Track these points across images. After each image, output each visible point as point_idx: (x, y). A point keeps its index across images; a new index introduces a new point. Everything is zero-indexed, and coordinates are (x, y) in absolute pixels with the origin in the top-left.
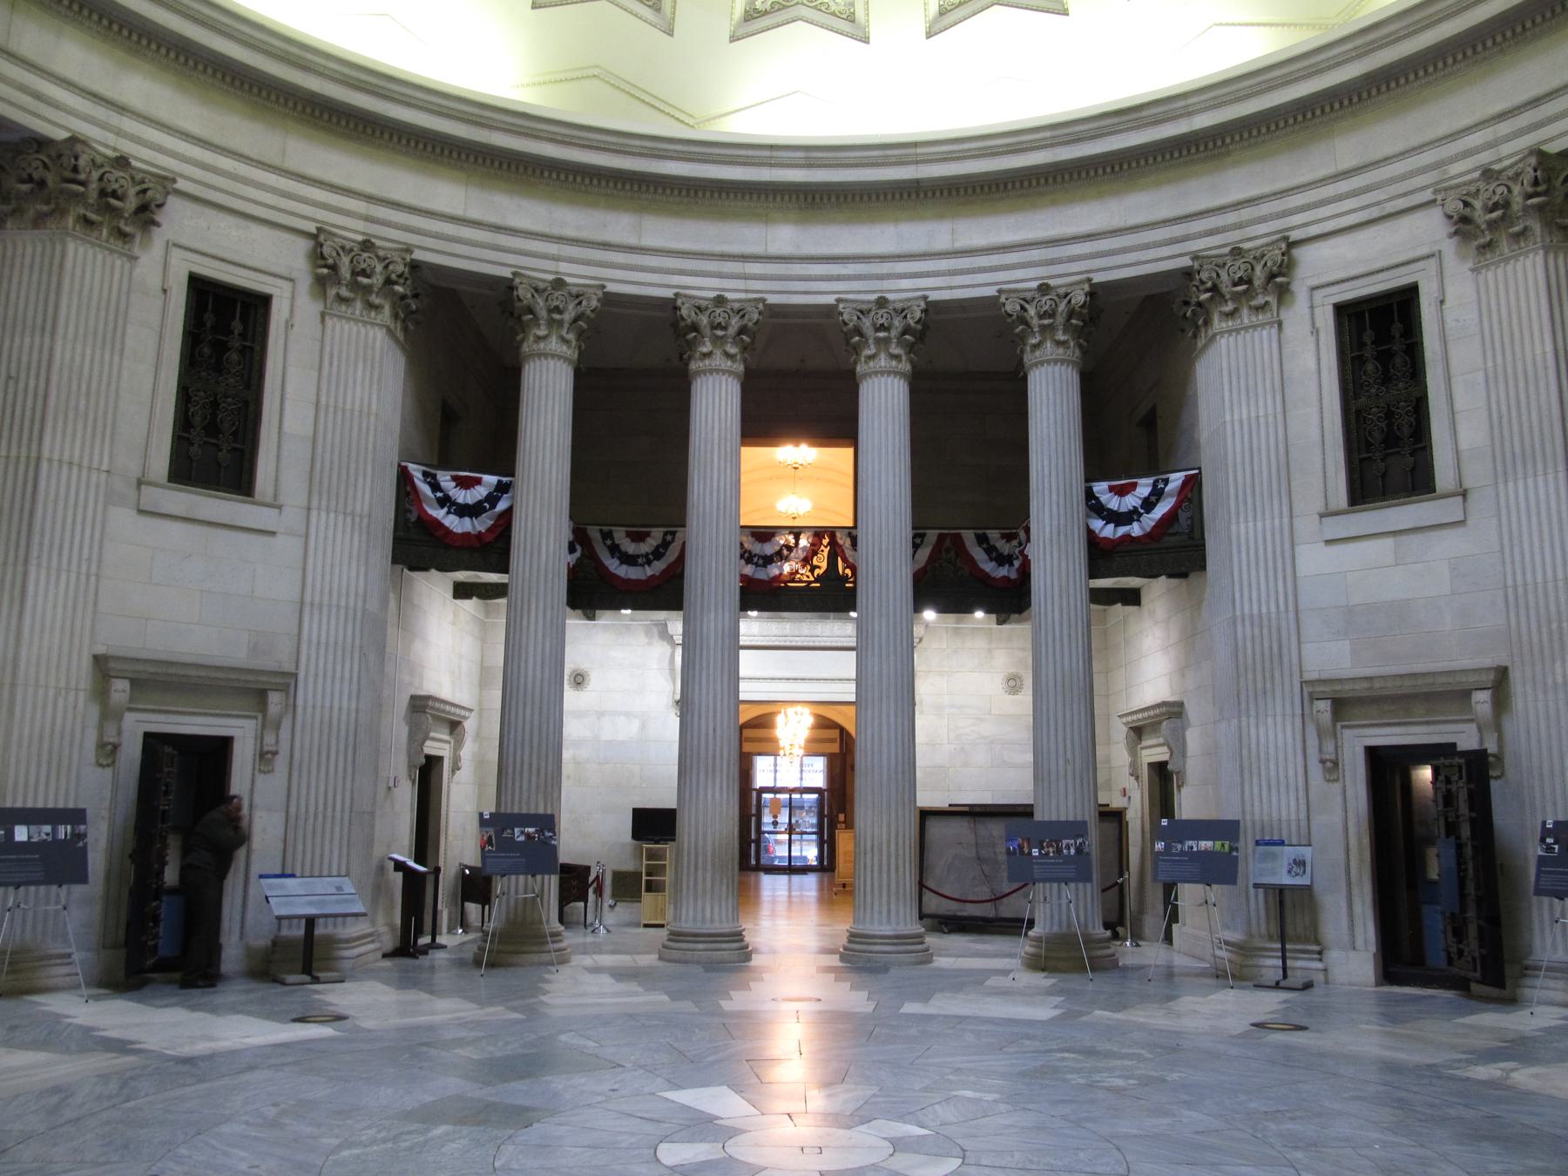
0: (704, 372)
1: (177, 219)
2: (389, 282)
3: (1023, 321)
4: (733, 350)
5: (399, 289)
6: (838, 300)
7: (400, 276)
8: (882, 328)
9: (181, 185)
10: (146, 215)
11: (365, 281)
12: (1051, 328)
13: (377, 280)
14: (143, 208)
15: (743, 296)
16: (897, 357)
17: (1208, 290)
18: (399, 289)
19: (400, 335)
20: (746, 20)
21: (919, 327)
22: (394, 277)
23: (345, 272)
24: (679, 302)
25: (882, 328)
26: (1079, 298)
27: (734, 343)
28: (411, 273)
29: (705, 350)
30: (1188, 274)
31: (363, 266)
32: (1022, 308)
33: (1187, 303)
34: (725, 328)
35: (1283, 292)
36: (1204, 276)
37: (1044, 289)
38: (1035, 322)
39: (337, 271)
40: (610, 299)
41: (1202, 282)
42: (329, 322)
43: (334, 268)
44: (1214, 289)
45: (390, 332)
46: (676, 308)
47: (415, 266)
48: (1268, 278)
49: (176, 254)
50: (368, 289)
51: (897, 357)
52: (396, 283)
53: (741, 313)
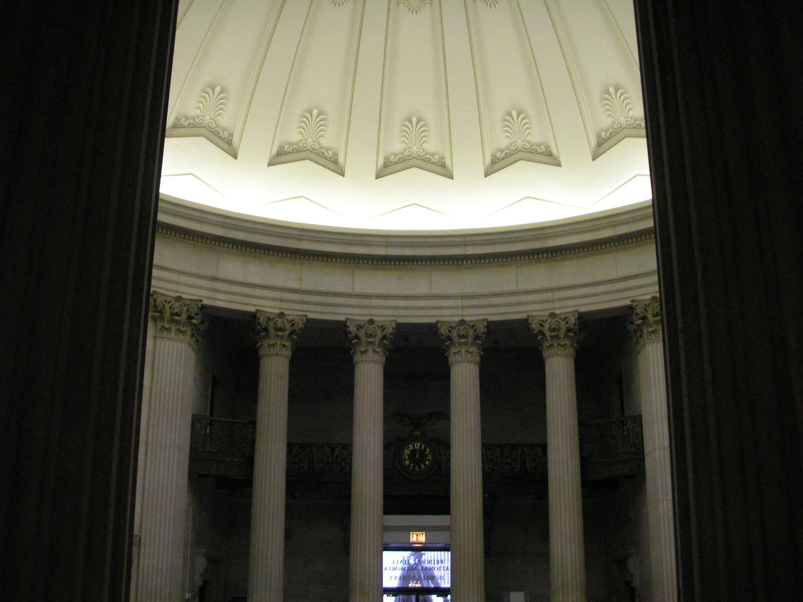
2: (190, 318)
3: (541, 333)
4: (378, 350)
5: (194, 321)
6: (438, 322)
7: (196, 314)
8: (463, 337)
11: (177, 318)
12: (557, 337)
13: (184, 317)
17: (641, 319)
18: (194, 321)
19: (195, 347)
20: (384, 167)
21: (485, 336)
22: (192, 315)
23: (167, 315)
24: (348, 324)
25: (463, 337)
26: (572, 320)
27: (379, 346)
28: (201, 311)
29: (363, 349)
30: (630, 308)
31: (176, 310)
32: (541, 325)
33: (632, 323)
34: (374, 337)
36: (638, 311)
37: (552, 315)
38: (548, 334)
40: (309, 320)
41: (637, 314)
42: (158, 342)
43: (161, 312)
44: (644, 318)
45: (189, 343)
46: (345, 325)
47: (204, 307)
50: (178, 322)
52: (193, 318)
53: (383, 328)
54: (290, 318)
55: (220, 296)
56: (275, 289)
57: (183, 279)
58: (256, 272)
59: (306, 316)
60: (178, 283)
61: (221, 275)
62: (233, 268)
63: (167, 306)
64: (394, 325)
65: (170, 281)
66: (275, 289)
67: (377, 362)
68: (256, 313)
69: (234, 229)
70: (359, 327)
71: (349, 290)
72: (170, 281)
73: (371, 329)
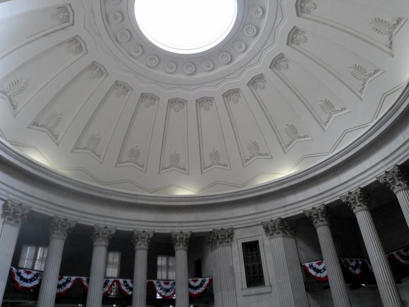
0: (357, 212)
1: (237, 233)
9: (234, 227)
10: (232, 234)
14: (229, 236)
15: (318, 205)
16: (322, 221)
35: (232, 239)
39: (269, 229)
48: (227, 236)
49: (239, 240)
51: (322, 221)
54: (318, 208)
55: (289, 212)
56: (309, 199)
57: (273, 212)
58: (300, 196)
59: (324, 204)
60: (272, 215)
61: (287, 204)
62: (291, 199)
63: (269, 225)
64: (360, 190)
65: (268, 215)
66: (309, 199)
67: (362, 210)
68: (303, 213)
69: (282, 184)
70: (347, 198)
71: (339, 183)
72: (268, 215)
73: (352, 196)
